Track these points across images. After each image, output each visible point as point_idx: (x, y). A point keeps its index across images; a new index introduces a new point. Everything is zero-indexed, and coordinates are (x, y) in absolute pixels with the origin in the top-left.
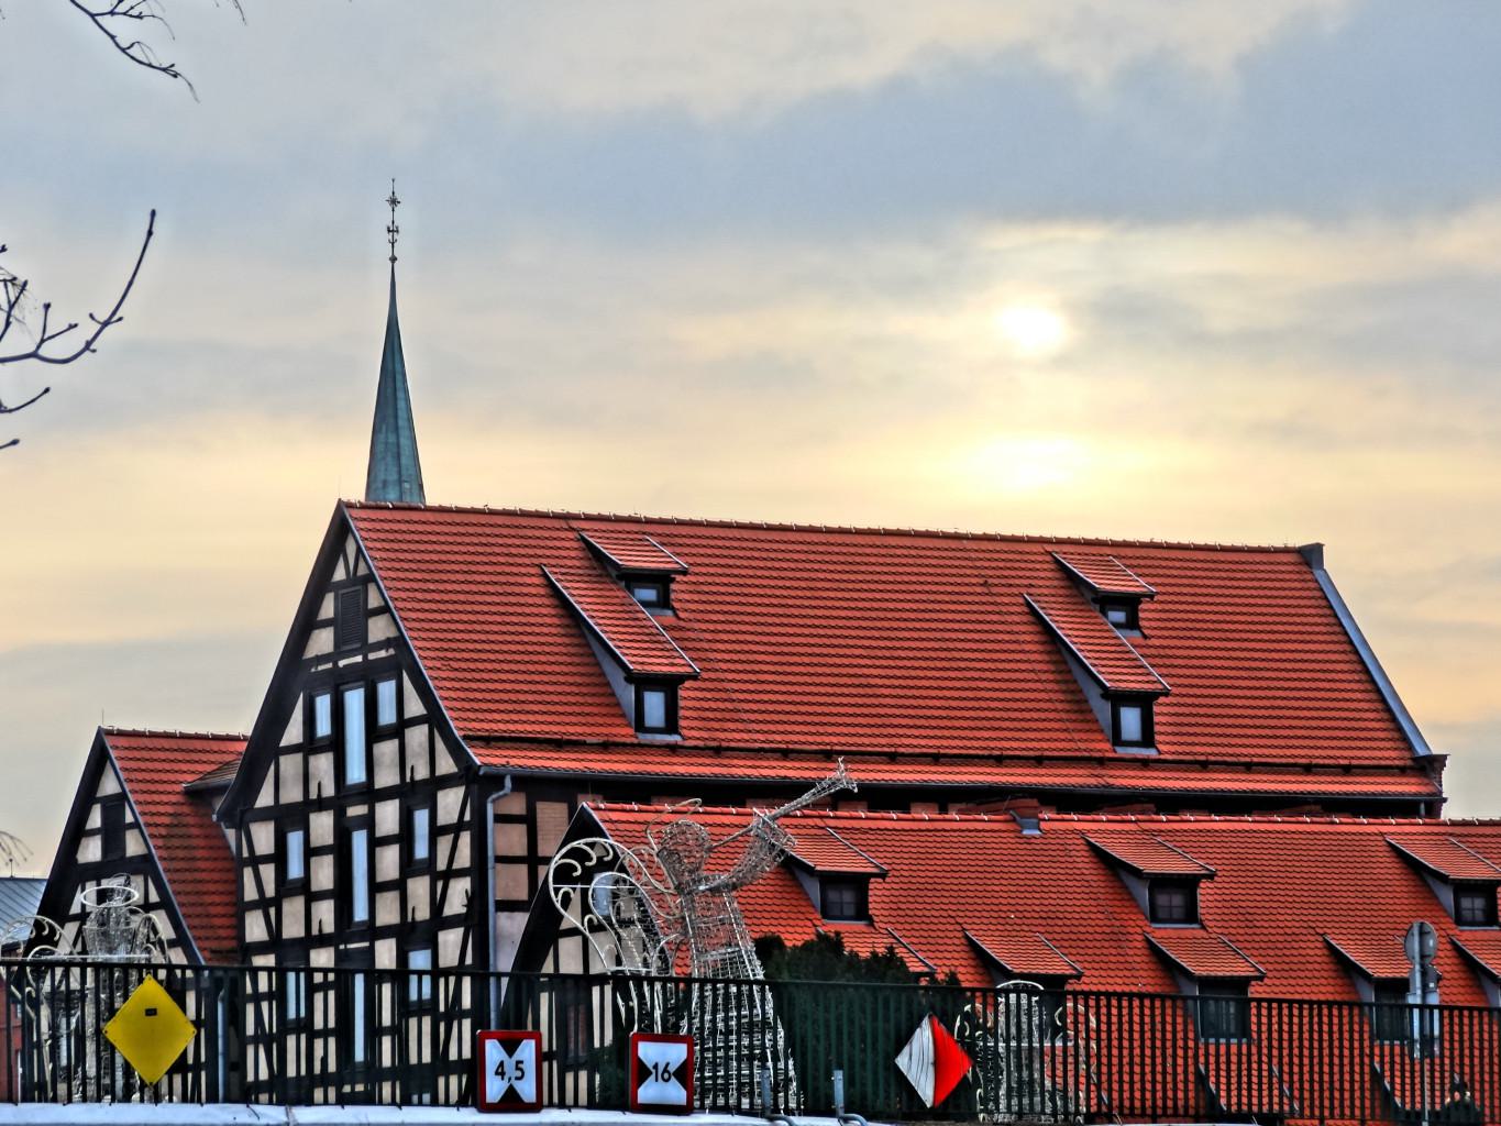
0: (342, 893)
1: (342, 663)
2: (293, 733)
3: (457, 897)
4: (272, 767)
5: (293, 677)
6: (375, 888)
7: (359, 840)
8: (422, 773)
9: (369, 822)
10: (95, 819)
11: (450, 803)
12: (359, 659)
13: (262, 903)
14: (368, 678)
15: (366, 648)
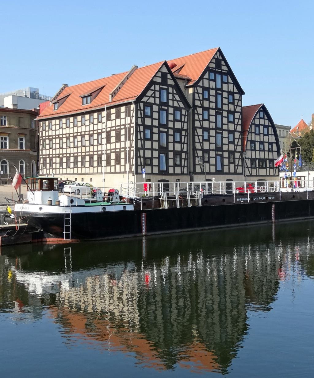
0: (216, 102)
1: (217, 70)
2: (206, 76)
3: (238, 109)
4: (202, 80)
5: (208, 69)
6: (222, 104)
7: (219, 97)
8: (232, 91)
9: (222, 94)
10: (159, 74)
11: (237, 96)
12: (220, 71)
13: (199, 100)
14: (222, 74)
15: (222, 70)
